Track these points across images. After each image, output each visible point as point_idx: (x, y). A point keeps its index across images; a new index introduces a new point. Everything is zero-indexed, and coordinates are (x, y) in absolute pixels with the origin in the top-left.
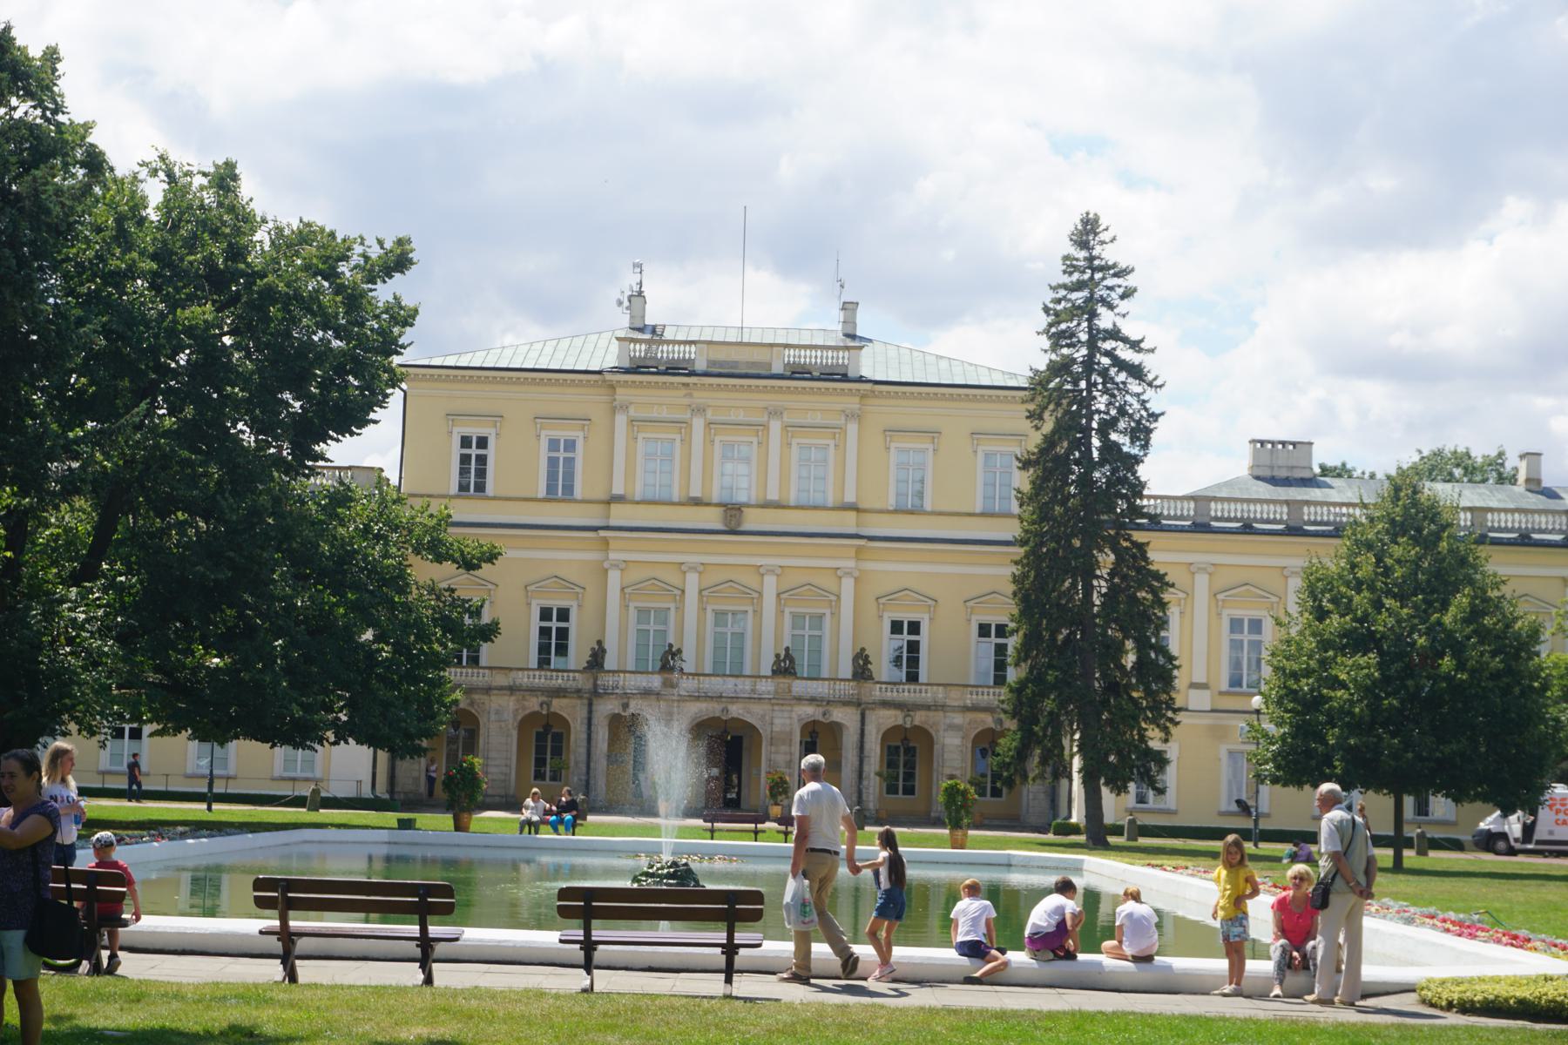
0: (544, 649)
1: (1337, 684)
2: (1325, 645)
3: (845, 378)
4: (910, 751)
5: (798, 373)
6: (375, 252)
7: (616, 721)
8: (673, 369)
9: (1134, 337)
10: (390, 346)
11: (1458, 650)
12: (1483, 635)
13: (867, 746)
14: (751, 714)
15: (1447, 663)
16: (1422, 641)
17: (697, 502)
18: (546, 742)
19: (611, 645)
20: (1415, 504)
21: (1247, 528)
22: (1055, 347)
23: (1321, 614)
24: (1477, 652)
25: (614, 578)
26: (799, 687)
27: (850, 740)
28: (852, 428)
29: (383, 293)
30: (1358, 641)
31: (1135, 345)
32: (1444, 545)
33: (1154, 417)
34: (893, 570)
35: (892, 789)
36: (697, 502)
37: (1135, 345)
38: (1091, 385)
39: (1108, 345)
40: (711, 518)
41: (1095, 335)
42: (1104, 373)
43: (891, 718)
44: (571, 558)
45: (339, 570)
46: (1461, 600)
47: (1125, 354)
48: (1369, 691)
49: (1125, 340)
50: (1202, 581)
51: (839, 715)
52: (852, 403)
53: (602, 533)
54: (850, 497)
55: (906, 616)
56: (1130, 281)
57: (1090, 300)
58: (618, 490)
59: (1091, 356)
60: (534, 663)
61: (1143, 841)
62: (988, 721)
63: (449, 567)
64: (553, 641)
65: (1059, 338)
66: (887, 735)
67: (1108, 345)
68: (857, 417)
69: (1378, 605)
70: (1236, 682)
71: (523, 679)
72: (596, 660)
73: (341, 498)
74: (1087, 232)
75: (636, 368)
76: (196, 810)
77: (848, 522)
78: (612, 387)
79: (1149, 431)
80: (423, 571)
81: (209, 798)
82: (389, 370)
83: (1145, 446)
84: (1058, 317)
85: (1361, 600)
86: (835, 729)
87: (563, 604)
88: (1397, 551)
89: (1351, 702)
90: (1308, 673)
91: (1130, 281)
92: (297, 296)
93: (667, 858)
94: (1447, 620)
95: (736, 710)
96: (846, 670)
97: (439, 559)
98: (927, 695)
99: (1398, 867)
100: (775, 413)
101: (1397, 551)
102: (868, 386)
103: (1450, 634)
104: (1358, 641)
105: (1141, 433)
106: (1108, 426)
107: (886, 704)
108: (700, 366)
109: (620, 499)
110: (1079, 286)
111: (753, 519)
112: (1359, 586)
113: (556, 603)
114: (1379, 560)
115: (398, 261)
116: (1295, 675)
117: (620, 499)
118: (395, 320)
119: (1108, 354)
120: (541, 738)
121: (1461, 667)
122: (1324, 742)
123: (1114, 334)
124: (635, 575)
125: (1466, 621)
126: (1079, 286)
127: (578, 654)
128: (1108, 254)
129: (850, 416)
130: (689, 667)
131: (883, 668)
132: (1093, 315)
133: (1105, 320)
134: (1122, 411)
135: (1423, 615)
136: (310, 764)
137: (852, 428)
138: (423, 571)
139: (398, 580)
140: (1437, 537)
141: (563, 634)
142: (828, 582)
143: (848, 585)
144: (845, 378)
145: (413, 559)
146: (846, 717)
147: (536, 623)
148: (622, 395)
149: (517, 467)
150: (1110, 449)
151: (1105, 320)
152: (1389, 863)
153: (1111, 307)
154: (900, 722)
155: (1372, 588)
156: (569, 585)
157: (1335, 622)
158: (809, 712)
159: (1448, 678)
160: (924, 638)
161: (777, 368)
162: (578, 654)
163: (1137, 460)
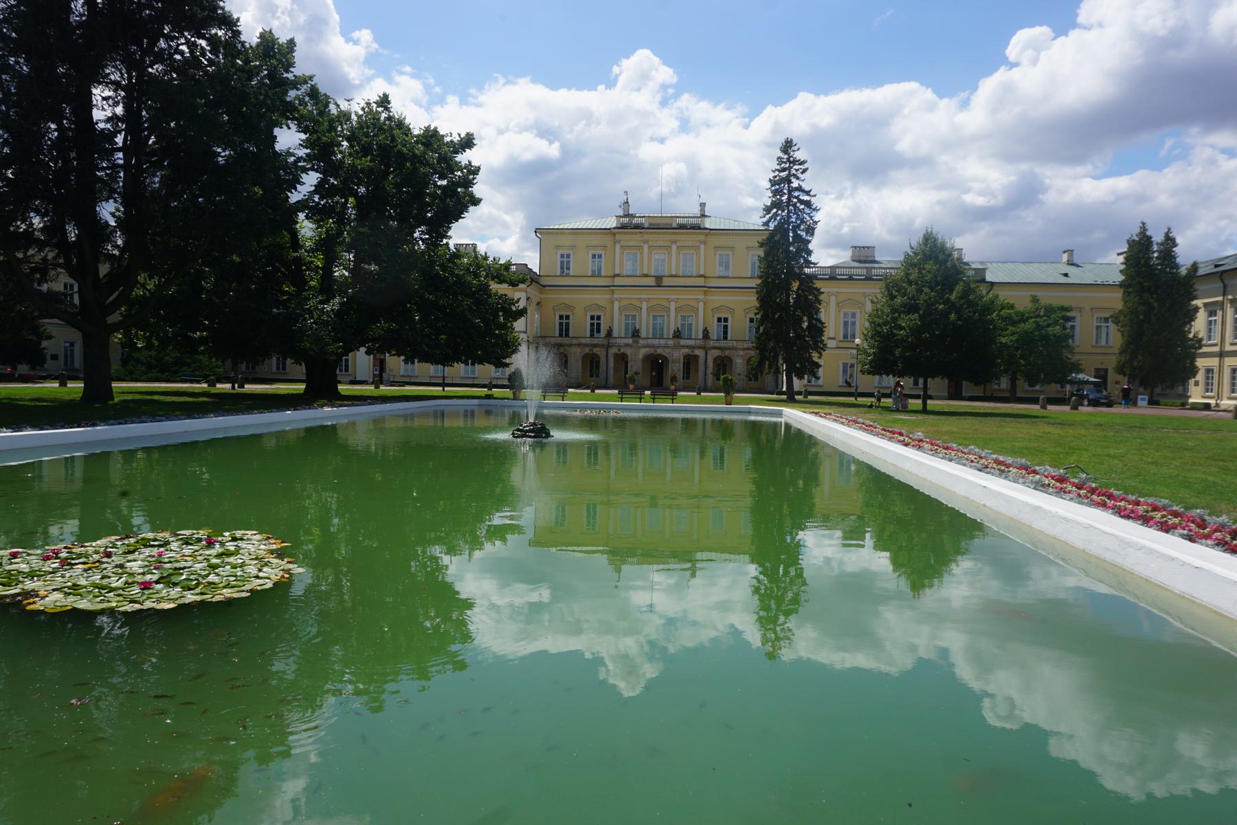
0: (592, 330)
1: (902, 328)
2: (894, 311)
3: (699, 228)
4: (725, 366)
5: (682, 227)
6: (456, 139)
7: (616, 355)
8: (637, 227)
9: (807, 189)
10: (467, 183)
11: (958, 311)
12: (971, 304)
14: (666, 352)
15: (953, 316)
16: (941, 307)
17: (646, 276)
20: (935, 245)
21: (851, 278)
23: (892, 297)
25: (616, 305)
26: (683, 342)
27: (701, 361)
28: (702, 247)
29: (463, 158)
30: (911, 308)
31: (808, 193)
32: (949, 264)
33: (816, 223)
34: (717, 299)
36: (646, 276)
37: (808, 193)
39: (796, 194)
40: (651, 281)
41: (791, 191)
42: (794, 206)
43: (716, 353)
44: (601, 298)
45: (461, 287)
48: (916, 331)
49: (804, 191)
50: (833, 299)
51: (697, 352)
52: (702, 238)
54: (702, 273)
55: (723, 316)
57: (789, 175)
58: (617, 272)
59: (789, 199)
61: (810, 398)
63: (505, 286)
64: (595, 328)
65: (775, 193)
66: (715, 359)
67: (796, 194)
68: (704, 243)
69: (920, 291)
70: (845, 336)
71: (583, 341)
72: (609, 333)
73: (457, 255)
75: (623, 227)
77: (701, 282)
78: (614, 234)
80: (494, 286)
81: (444, 385)
82: (472, 196)
83: (812, 235)
84: (773, 182)
85: (911, 290)
86: (696, 357)
88: (928, 267)
89: (907, 337)
90: (886, 323)
92: (415, 156)
93: (531, 420)
94: (953, 297)
95: (659, 351)
96: (701, 336)
97: (501, 283)
98: (730, 344)
99: (925, 411)
100: (674, 242)
101: (928, 267)
104: (911, 308)
105: (811, 231)
106: (799, 226)
107: (715, 348)
108: (646, 225)
109: (618, 275)
111: (666, 281)
112: (910, 283)
113: (596, 314)
114: (920, 272)
115: (467, 142)
116: (879, 325)
117: (618, 275)
119: (796, 197)
120: (592, 362)
121: (959, 318)
122: (894, 355)
123: (800, 189)
125: (961, 298)
126: (784, 170)
128: (799, 155)
129: (701, 242)
130: (643, 334)
131: (714, 334)
132: (790, 182)
133: (795, 184)
134: (803, 221)
137: (702, 247)
138: (494, 286)
140: (946, 261)
141: (599, 325)
143: (701, 305)
144: (699, 228)
147: (589, 321)
148: (618, 237)
149: (582, 264)
150: (797, 237)
151: (795, 184)
152: (920, 407)
153: (798, 178)
155: (916, 284)
157: (899, 300)
160: (729, 324)
163: (809, 242)
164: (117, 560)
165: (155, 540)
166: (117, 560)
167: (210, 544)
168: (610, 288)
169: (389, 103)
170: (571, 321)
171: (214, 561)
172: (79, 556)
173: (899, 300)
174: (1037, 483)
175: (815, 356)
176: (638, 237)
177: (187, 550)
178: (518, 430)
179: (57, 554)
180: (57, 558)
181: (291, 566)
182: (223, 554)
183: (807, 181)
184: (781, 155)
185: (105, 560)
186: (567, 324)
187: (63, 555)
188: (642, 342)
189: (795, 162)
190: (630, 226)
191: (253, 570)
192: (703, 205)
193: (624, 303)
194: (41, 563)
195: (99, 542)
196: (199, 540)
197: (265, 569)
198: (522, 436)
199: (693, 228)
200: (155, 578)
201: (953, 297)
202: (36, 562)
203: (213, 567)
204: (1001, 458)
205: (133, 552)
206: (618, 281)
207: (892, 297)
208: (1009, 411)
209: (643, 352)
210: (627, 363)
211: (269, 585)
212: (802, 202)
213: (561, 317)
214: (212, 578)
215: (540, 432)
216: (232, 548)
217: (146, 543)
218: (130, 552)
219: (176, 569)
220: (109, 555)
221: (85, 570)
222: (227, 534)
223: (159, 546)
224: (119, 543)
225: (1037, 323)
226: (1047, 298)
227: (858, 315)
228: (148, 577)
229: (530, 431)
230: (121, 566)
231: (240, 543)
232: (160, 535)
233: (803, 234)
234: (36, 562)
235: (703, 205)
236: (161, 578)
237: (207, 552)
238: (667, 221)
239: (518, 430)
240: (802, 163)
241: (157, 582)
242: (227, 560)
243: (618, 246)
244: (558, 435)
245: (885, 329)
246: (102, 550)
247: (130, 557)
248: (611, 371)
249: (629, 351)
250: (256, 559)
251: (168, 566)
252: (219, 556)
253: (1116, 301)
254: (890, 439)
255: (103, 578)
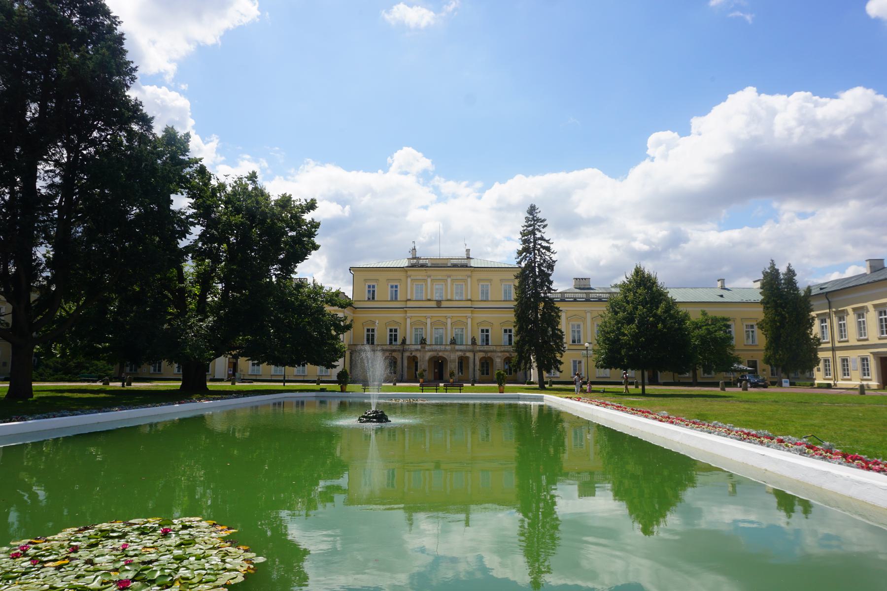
0: (391, 340)
1: (624, 335)
2: (618, 322)
4: (487, 364)
5: (455, 266)
7: (409, 357)
8: (422, 266)
10: (311, 235)
11: (664, 322)
12: (672, 317)
17: (429, 300)
21: (575, 300)
22: (524, 243)
23: (616, 313)
24: (670, 322)
25: (408, 321)
26: (457, 347)
27: (471, 361)
28: (469, 280)
29: (307, 217)
30: (630, 320)
31: (547, 241)
33: (554, 262)
34: (481, 316)
35: (483, 374)
36: (429, 300)
37: (547, 241)
38: (535, 254)
39: (540, 242)
40: (434, 304)
41: (535, 240)
42: (539, 250)
43: (481, 355)
44: (397, 316)
46: (663, 305)
47: (545, 244)
48: (635, 337)
49: (544, 240)
51: (468, 354)
52: (469, 273)
55: (485, 328)
56: (545, 223)
57: (534, 229)
58: (409, 298)
59: (534, 245)
62: (508, 355)
63: (336, 308)
64: (393, 338)
65: (525, 242)
66: (481, 360)
68: (470, 276)
71: (385, 347)
74: (532, 210)
75: (413, 266)
76: (279, 386)
77: (469, 304)
78: (406, 271)
79: (553, 266)
80: (328, 308)
81: (284, 381)
83: (552, 270)
85: (629, 307)
86: (467, 358)
90: (613, 331)
91: (545, 223)
92: (274, 214)
93: (374, 409)
94: (659, 311)
95: (440, 354)
96: (470, 343)
97: (333, 305)
98: (491, 348)
99: (643, 394)
100: (449, 276)
101: (639, 291)
103: (660, 317)
104: (630, 320)
105: (551, 266)
107: (480, 351)
110: (530, 226)
111: (444, 304)
112: (628, 302)
113: (393, 328)
114: (634, 295)
115: (311, 206)
116: (608, 333)
118: (312, 227)
121: (665, 327)
122: (620, 353)
123: (542, 239)
125: (664, 312)
126: (530, 226)
127: (399, 341)
129: (468, 276)
130: (428, 342)
132: (534, 234)
133: (538, 235)
134: (544, 261)
135: (650, 310)
136: (303, 371)
137: (469, 280)
138: (328, 308)
139: (321, 310)
141: (396, 335)
142: (465, 320)
143: (469, 321)
145: (325, 305)
146: (469, 355)
148: (409, 273)
149: (383, 293)
150: (541, 271)
151: (538, 235)
155: (632, 303)
156: (397, 323)
157: (621, 315)
158: (460, 354)
159: (660, 331)
160: (490, 334)
161: (449, 265)
162: (399, 341)
163: (550, 275)
164: (84, 554)
165: (113, 531)
166: (84, 554)
167: (166, 534)
169: (256, 177)
171: (178, 552)
172: (50, 551)
173: (621, 315)
174: (801, 450)
175: (558, 355)
176: (424, 273)
177: (147, 541)
178: (363, 417)
179: (25, 551)
180: (26, 555)
181: (250, 555)
182: (181, 544)
183: (547, 233)
184: (528, 215)
185: (72, 555)
186: (373, 335)
187: (31, 551)
188: (427, 348)
189: (538, 220)
190: (417, 265)
191: (216, 560)
192: (468, 251)
193: (434, 320)
194: (11, 562)
195: (60, 535)
196: (155, 530)
197: (228, 560)
198: (367, 421)
199: (462, 266)
200: (131, 575)
201: (659, 311)
202: (7, 563)
203: (180, 559)
204: (746, 431)
205: (96, 545)
206: (409, 304)
207: (616, 313)
208: (709, 393)
209: (428, 355)
210: (417, 363)
211: (240, 579)
212: (544, 248)
213: (391, 330)
214: (183, 572)
215: (381, 417)
216: (187, 537)
217: (106, 535)
218: (92, 546)
219: (144, 563)
220: (75, 549)
221: (58, 568)
222: (175, 521)
223: (119, 537)
224: (80, 535)
225: (707, 329)
226: (713, 312)
227: (582, 326)
228: (124, 576)
229: (373, 417)
230: (90, 562)
231: (193, 531)
232: (116, 525)
233: (546, 269)
234: (7, 563)
235: (468, 251)
236: (136, 576)
237: (167, 542)
238: (445, 262)
239: (363, 417)
240: (544, 220)
241: (133, 580)
242: (190, 550)
243: (409, 280)
244: (395, 420)
245: (612, 335)
246: (66, 543)
247: (96, 551)
248: (405, 369)
249: (418, 355)
250: (214, 548)
251: (135, 559)
252: (178, 546)
253: (759, 314)
254: (646, 417)
255: (78, 577)
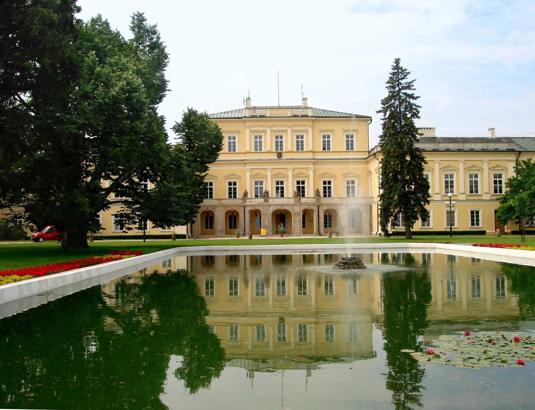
13: (320, 215)
14: (289, 208)
18: (232, 219)
19: (248, 191)
34: (324, 168)
43: (326, 208)
51: (312, 207)
52: (310, 123)
53: (244, 161)
54: (310, 148)
58: (248, 149)
60: (227, 197)
66: (325, 212)
72: (246, 194)
77: (310, 156)
87: (235, 181)
102: (314, 118)
108: (268, 115)
111: (285, 156)
120: (230, 217)
124: (255, 172)
129: (309, 127)
130: (270, 197)
141: (235, 189)
143: (311, 173)
144: (307, 116)
147: (227, 186)
154: (329, 208)
161: (289, 115)
162: (239, 195)
168: (244, 162)
170: (214, 187)
188: (270, 201)
243: (248, 131)
249: (261, 208)
